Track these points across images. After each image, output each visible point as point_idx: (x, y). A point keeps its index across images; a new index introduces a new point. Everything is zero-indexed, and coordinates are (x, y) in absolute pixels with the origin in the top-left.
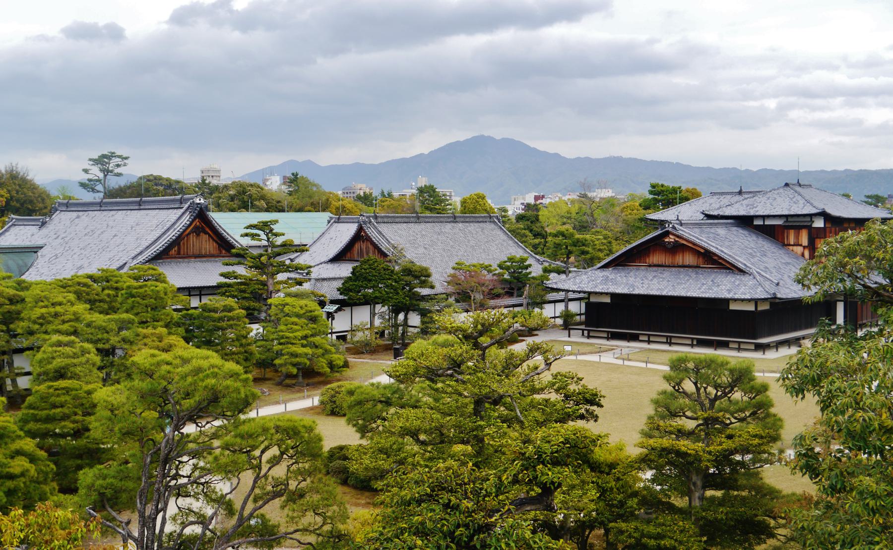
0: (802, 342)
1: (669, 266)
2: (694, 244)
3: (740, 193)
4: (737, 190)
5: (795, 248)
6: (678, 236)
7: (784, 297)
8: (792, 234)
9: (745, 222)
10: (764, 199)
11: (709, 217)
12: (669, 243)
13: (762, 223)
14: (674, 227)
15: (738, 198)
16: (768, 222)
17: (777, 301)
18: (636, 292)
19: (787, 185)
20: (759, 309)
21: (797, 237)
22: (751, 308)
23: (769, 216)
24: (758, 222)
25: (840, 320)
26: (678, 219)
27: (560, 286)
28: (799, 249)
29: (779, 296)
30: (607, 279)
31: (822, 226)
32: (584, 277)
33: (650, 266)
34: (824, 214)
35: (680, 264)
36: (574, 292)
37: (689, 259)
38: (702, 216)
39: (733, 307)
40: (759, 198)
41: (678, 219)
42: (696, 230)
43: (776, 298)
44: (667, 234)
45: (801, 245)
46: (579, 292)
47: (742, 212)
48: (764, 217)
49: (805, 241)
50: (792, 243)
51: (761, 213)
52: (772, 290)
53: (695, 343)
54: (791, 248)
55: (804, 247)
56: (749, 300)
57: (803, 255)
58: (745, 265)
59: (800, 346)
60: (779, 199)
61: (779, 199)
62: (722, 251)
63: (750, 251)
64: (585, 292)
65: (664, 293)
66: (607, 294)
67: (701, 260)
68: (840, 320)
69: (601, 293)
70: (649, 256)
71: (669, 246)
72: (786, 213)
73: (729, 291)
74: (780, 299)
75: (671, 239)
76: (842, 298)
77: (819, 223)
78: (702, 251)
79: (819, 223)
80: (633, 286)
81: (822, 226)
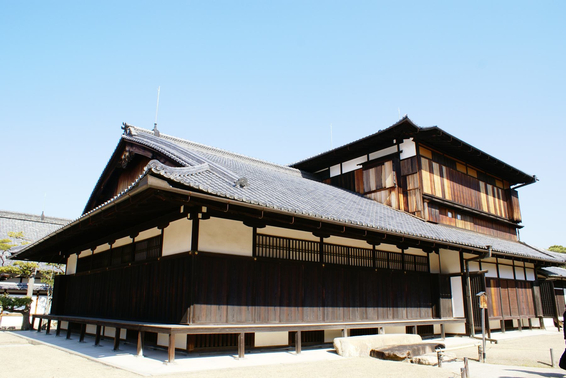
8: (372, 171)
20: (203, 246)
45: (385, 189)
50: (373, 188)
76: (458, 270)
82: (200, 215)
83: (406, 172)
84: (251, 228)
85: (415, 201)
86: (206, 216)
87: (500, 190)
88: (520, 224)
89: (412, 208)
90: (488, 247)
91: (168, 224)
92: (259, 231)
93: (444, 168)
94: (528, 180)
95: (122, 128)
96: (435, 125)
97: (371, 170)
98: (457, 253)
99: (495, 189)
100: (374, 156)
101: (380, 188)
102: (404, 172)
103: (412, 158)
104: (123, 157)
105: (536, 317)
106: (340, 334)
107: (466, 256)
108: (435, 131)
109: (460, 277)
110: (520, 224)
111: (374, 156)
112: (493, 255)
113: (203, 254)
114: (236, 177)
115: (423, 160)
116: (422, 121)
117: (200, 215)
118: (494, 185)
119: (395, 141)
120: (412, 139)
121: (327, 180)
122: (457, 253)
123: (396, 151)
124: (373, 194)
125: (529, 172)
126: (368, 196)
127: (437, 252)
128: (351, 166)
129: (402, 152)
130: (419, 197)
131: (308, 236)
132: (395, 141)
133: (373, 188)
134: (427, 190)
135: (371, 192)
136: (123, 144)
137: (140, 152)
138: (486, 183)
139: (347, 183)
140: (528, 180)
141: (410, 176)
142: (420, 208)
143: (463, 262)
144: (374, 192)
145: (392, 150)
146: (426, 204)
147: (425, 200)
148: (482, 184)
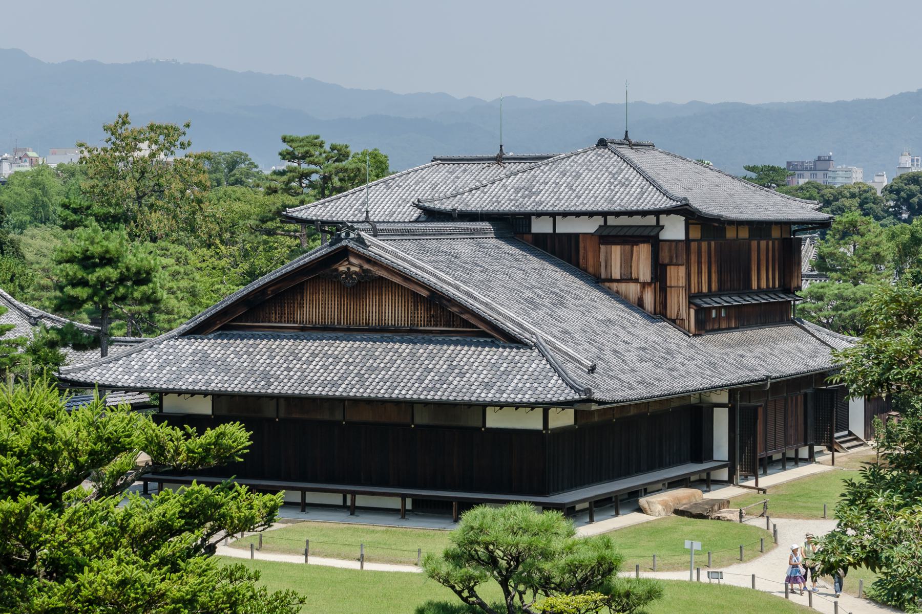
0: (643, 501)
1: (348, 330)
2: (407, 278)
3: (499, 159)
4: (495, 153)
5: (623, 287)
6: (368, 260)
7: (607, 397)
9: (512, 227)
10: (553, 176)
11: (431, 215)
12: (348, 273)
13: (551, 231)
14: (360, 241)
15: (494, 171)
16: (565, 227)
17: (594, 407)
18: (275, 389)
19: (602, 143)
20: (552, 425)
21: (627, 261)
22: (534, 422)
23: (565, 214)
24: (540, 227)
25: (721, 449)
26: (367, 220)
27: (93, 376)
28: (632, 290)
29: (597, 395)
30: (204, 361)
31: (682, 237)
32: (149, 354)
33: (303, 329)
34: (685, 211)
35: (374, 322)
36: (127, 390)
37: (394, 311)
38: (417, 213)
39: (494, 420)
40: (542, 172)
41: (367, 220)
42: (408, 244)
43: (590, 401)
44: (344, 254)
45: (636, 281)
46: (141, 390)
47: (506, 205)
48: (553, 215)
49: (644, 271)
50: (616, 274)
51: (549, 208)
52: (582, 379)
53: (409, 506)
54: (615, 286)
55: (644, 285)
56: (532, 406)
58: (520, 326)
59: (640, 510)
60: (586, 176)
61: (586, 176)
62: (471, 296)
63: (528, 294)
64: (152, 391)
65: (339, 392)
66: (205, 394)
67: (421, 313)
68: (721, 449)
69: (193, 393)
70: (301, 306)
72: (603, 206)
73: (488, 386)
74: (600, 403)
75: (354, 266)
78: (424, 293)
80: (266, 376)
81: (682, 237)
83: (667, 261)
85: (677, 302)
89: (672, 312)
93: (713, 243)
101: (628, 279)
102: (664, 256)
103: (677, 242)
105: (806, 445)
109: (725, 411)
123: (654, 223)
126: (607, 284)
129: (662, 227)
133: (616, 274)
146: (692, 312)
147: (692, 306)
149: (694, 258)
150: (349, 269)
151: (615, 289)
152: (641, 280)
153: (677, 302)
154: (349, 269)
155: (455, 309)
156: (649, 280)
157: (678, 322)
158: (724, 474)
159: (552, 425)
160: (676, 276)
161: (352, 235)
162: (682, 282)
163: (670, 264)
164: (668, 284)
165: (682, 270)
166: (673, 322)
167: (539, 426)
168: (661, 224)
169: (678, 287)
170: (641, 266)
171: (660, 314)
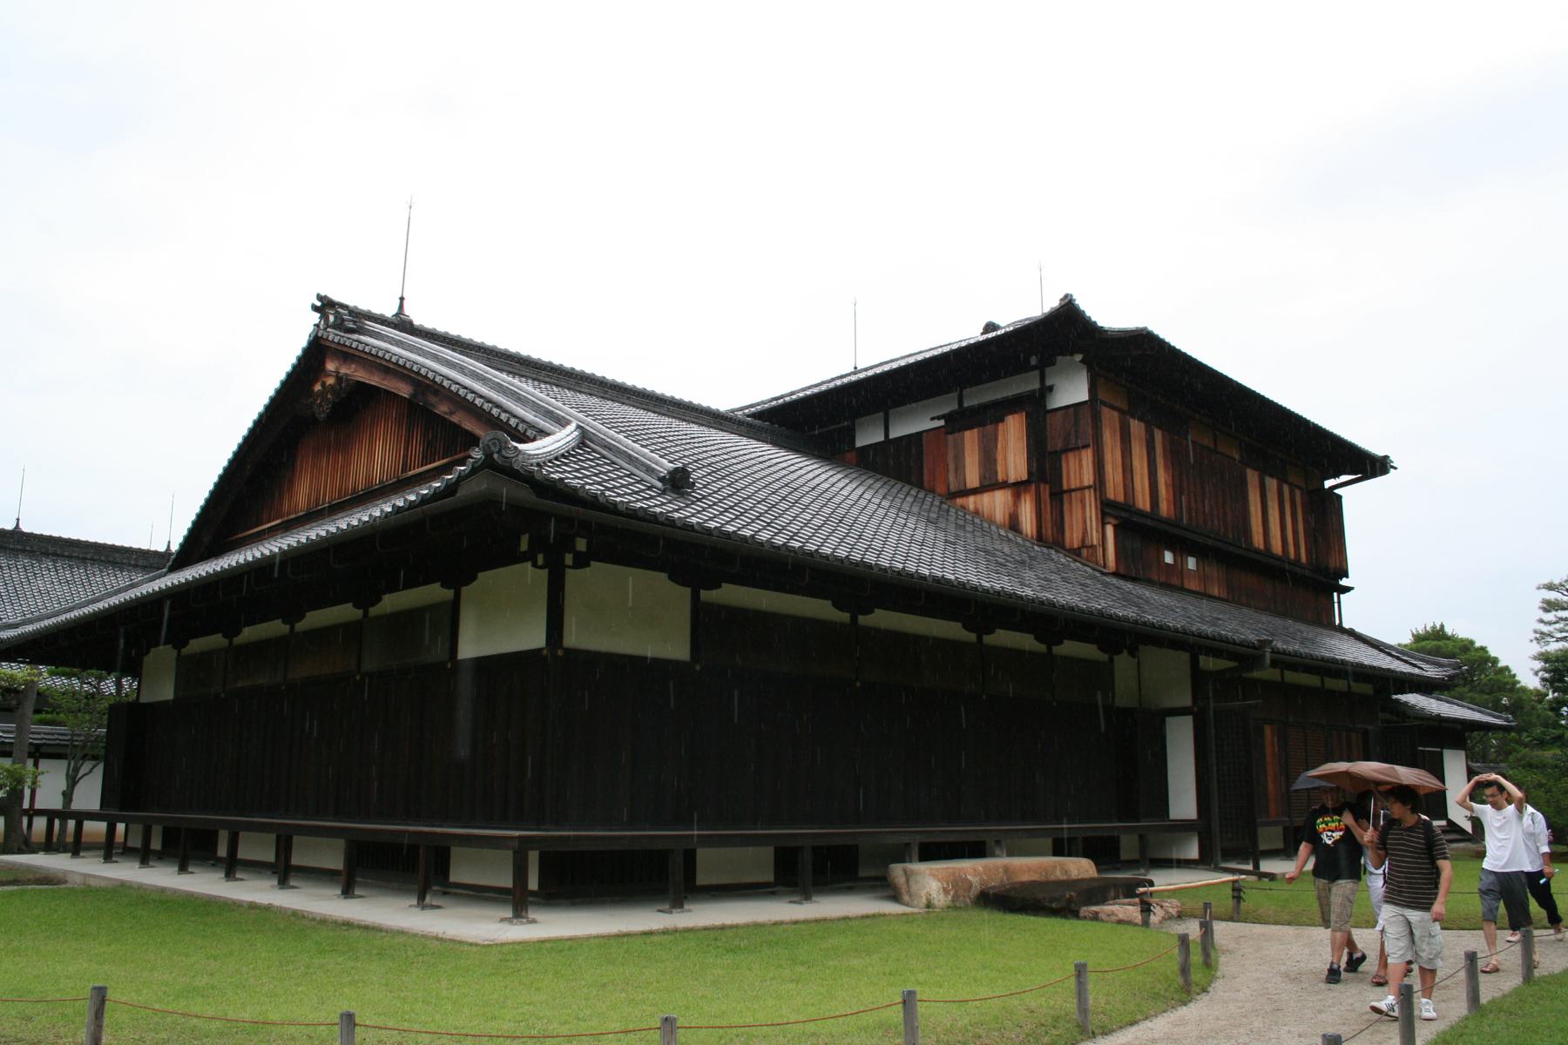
0: (897, 870)
13: (882, 438)
20: (573, 638)
24: (869, 436)
25: (1183, 803)
28: (997, 503)
45: (1004, 485)
49: (1014, 461)
54: (971, 501)
55: (1018, 488)
57: (1014, 524)
68: (1183, 803)
71: (322, 412)
76: (1186, 700)
77: (1072, 390)
78: (404, 390)
79: (1072, 390)
82: (569, 559)
83: (1060, 445)
84: (687, 591)
85: (1083, 521)
86: (582, 561)
87: (1298, 493)
88: (1344, 582)
89: (1073, 537)
90: (1264, 643)
91: (474, 578)
92: (705, 595)
93: (1158, 435)
94: (1370, 466)
95: (315, 308)
96: (1141, 325)
97: (967, 434)
98: (1185, 657)
99: (1286, 488)
100: (976, 397)
101: (990, 484)
104: (318, 387)
106: (901, 855)
107: (1209, 663)
108: (1143, 344)
110: (1344, 582)
111: (976, 397)
112: (1274, 664)
113: (571, 652)
114: (665, 466)
115: (1105, 411)
116: (1110, 313)
117: (569, 559)
118: (1282, 480)
119: (1034, 361)
120: (1079, 357)
121: (848, 455)
122: (1185, 657)
123: (1036, 386)
124: (971, 499)
125: (1378, 451)
126: (959, 501)
127: (1133, 652)
128: (915, 423)
129: (1051, 389)
130: (1092, 513)
131: (820, 609)
132: (1034, 361)
134: (1115, 491)
135: (967, 493)
136: (315, 353)
137: (374, 380)
138: (1264, 472)
139: (900, 466)
140: (1370, 466)
141: (1071, 455)
142: (1095, 538)
143: (1199, 679)
144: (975, 491)
145: (1025, 384)
146: (1110, 530)
148: (1252, 476)
149: (1110, 440)
150: (323, 384)
151: (972, 507)
152: (1012, 480)
153: (1083, 521)
154: (323, 384)
155: (442, 409)
156: (1025, 477)
157: (1084, 552)
158: (1193, 852)
159: (573, 638)
160: (1078, 469)
161: (332, 318)
162: (1088, 478)
163: (1067, 450)
164: (1065, 487)
165: (1087, 457)
166: (1075, 553)
167: (532, 637)
168: (1048, 383)
169: (1082, 489)
170: (1011, 458)
171: (1051, 536)
